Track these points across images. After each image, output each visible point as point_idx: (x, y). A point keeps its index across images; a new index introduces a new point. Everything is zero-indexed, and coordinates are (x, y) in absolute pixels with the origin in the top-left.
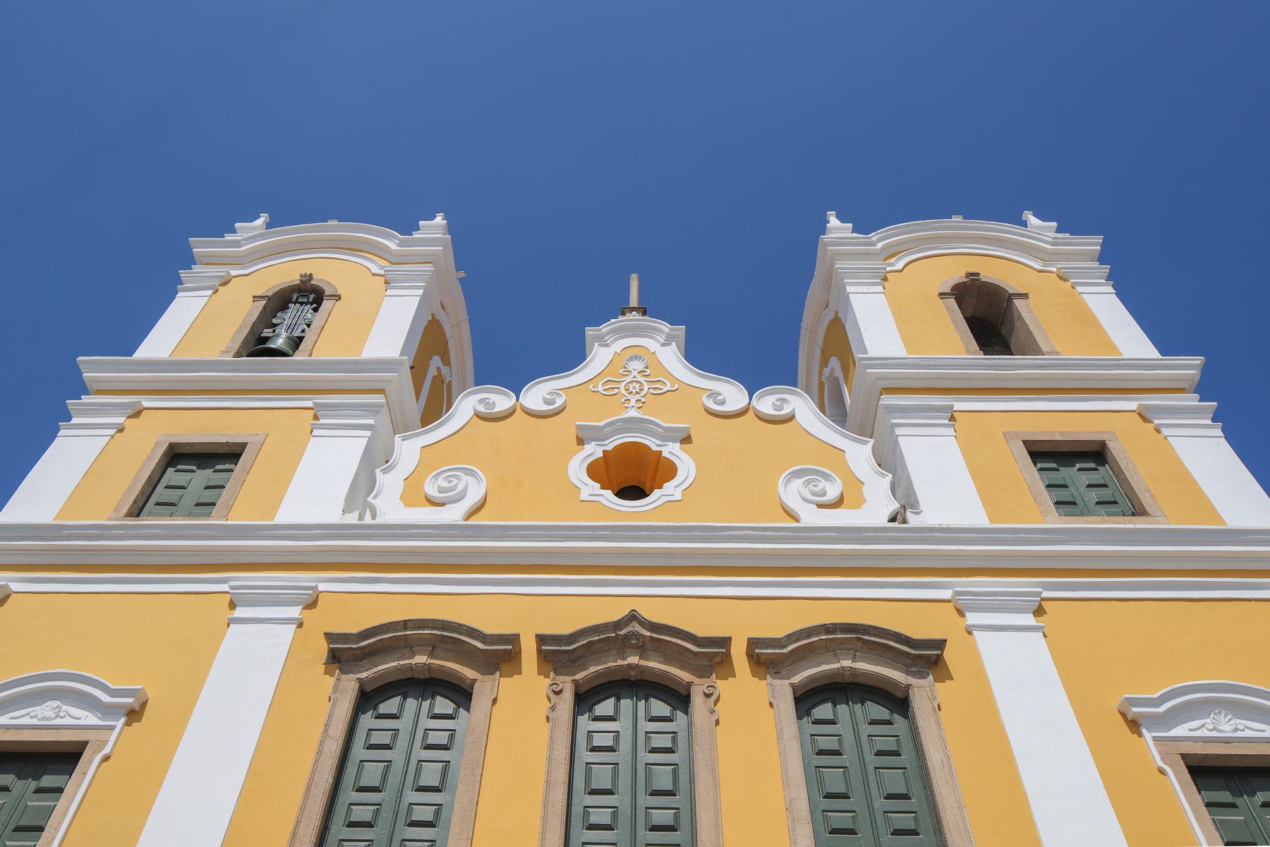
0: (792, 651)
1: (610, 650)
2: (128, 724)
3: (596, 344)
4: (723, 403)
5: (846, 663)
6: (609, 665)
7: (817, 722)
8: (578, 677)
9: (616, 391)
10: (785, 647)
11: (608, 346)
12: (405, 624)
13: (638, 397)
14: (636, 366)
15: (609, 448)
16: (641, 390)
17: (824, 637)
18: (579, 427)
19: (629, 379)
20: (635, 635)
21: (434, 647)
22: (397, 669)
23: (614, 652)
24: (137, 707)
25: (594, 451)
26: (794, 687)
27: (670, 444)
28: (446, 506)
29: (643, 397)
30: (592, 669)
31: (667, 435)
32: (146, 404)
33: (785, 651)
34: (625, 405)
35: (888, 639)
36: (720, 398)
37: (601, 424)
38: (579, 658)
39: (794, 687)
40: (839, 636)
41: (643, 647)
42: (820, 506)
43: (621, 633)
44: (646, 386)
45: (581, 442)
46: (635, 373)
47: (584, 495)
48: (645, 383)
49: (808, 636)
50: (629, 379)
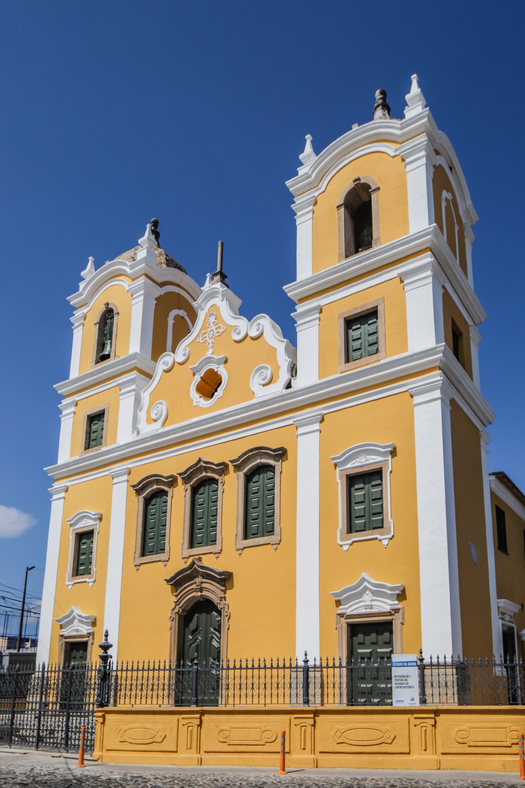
0: (242, 461)
1: (198, 472)
2: (100, 522)
3: (199, 310)
4: (239, 334)
5: (258, 461)
6: (199, 477)
7: (254, 483)
8: (191, 483)
9: (205, 339)
10: (238, 461)
11: (203, 309)
12: (148, 477)
13: (212, 340)
14: (212, 319)
15: (202, 375)
16: (213, 335)
17: (250, 454)
18: (192, 369)
19: (210, 329)
20: (201, 466)
21: (157, 482)
22: (151, 491)
23: (199, 472)
24: (100, 517)
25: (198, 378)
26: (244, 473)
27: (220, 366)
28: (158, 421)
29: (214, 340)
30: (195, 480)
31: (219, 362)
32: (77, 399)
33: (239, 463)
34: (208, 347)
35: (267, 450)
36: (238, 331)
37: (196, 365)
38: (190, 477)
39: (244, 473)
40: (255, 452)
41: (206, 469)
42: (264, 385)
43: (198, 466)
44: (215, 332)
45: (194, 374)
46: (212, 324)
47: (195, 404)
48: (215, 330)
49: (246, 455)
50: (210, 329)
